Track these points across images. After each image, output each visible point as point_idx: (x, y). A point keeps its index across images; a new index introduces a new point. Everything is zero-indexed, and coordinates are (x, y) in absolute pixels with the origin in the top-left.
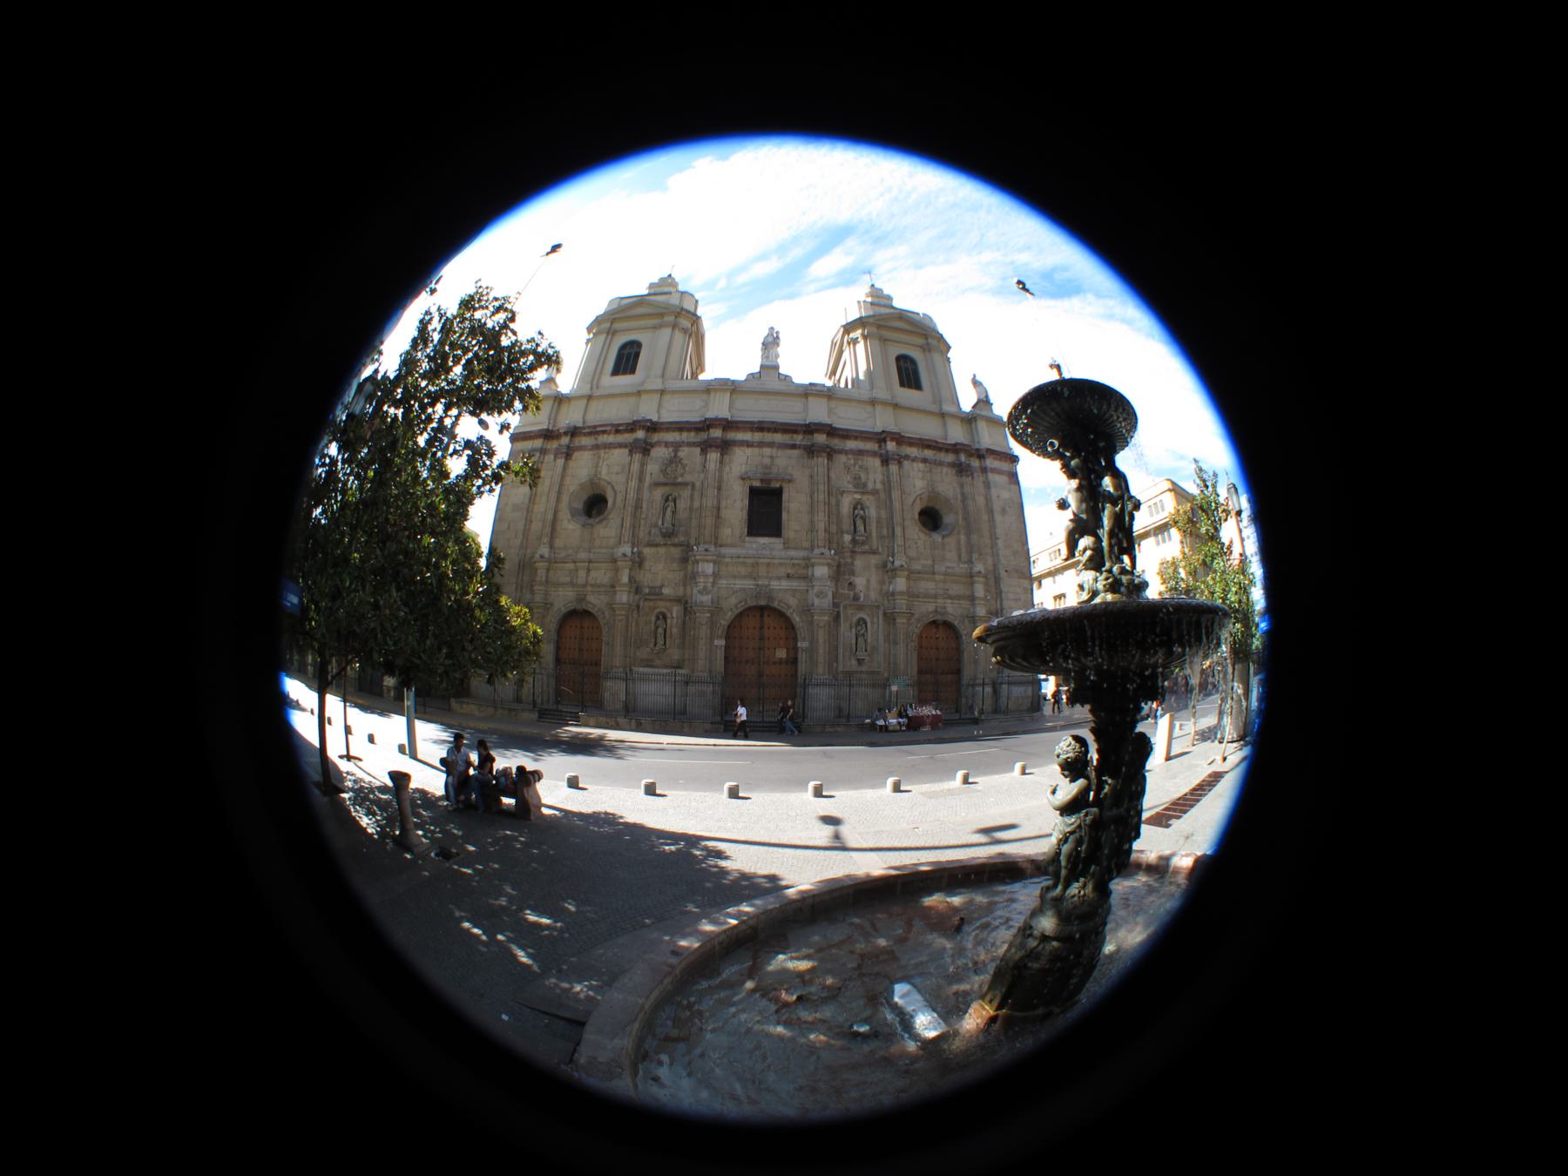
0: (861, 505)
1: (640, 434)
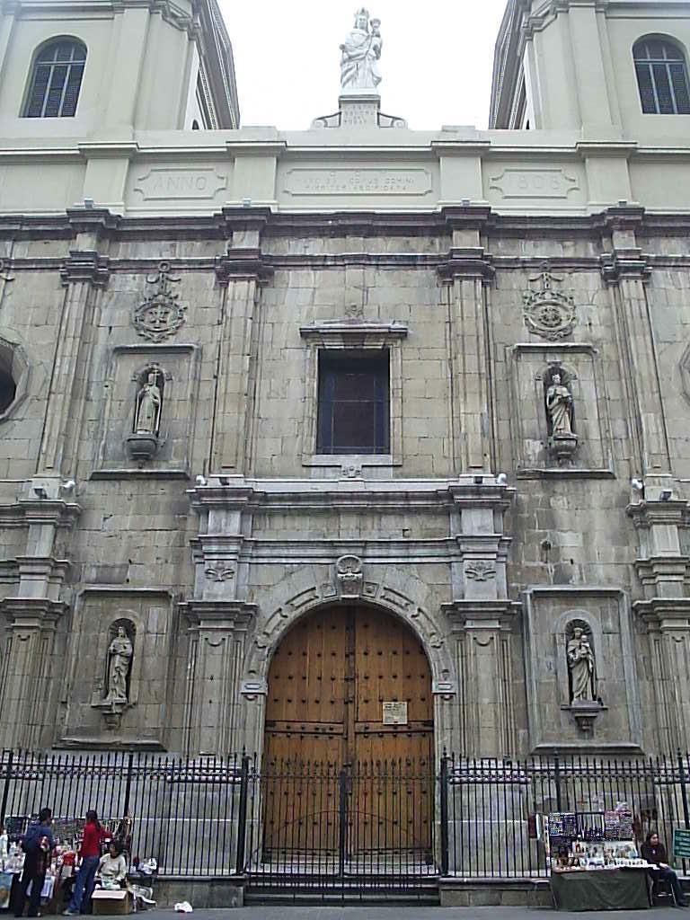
0: (562, 373)
1: (85, 243)
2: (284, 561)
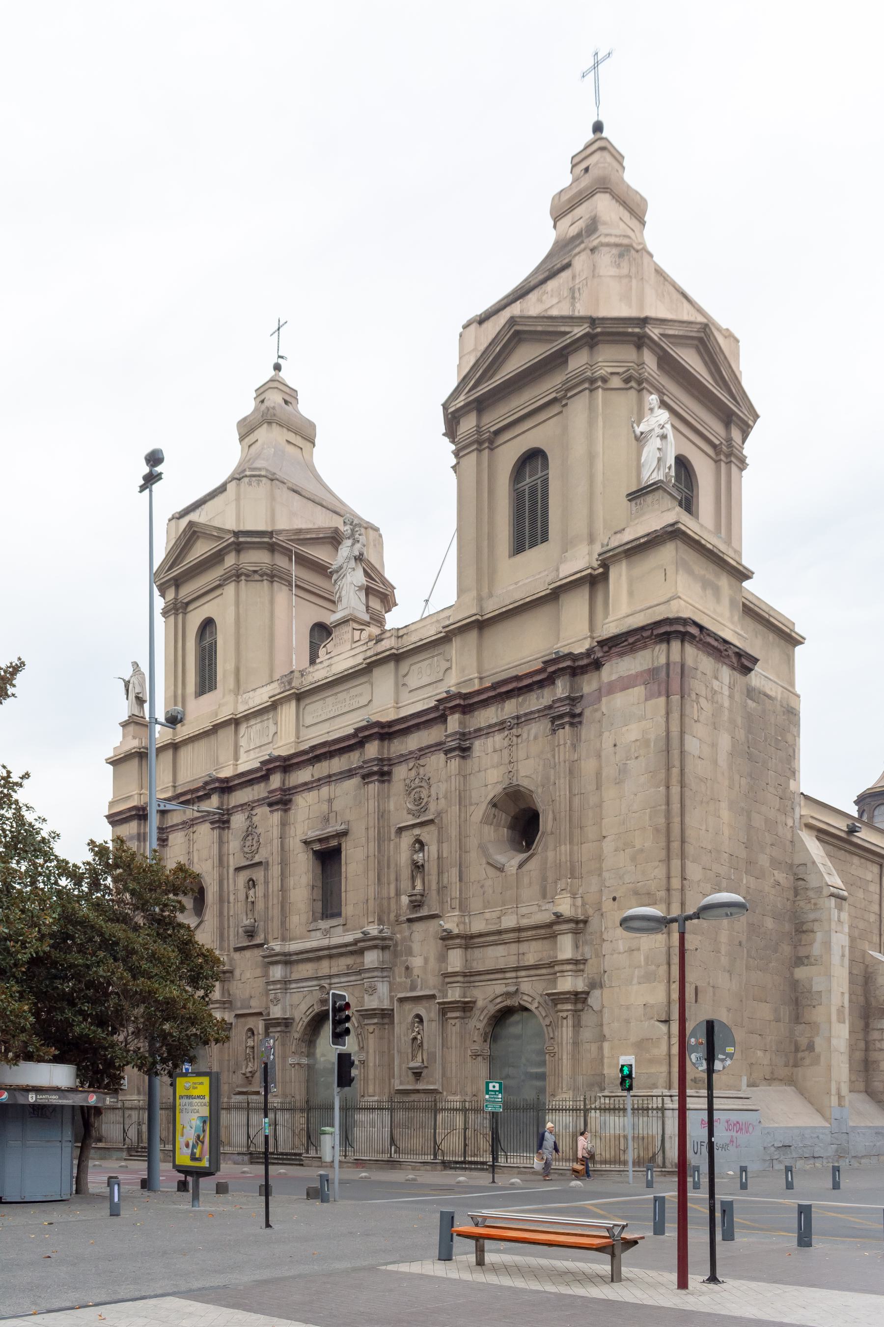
2: (302, 990)
